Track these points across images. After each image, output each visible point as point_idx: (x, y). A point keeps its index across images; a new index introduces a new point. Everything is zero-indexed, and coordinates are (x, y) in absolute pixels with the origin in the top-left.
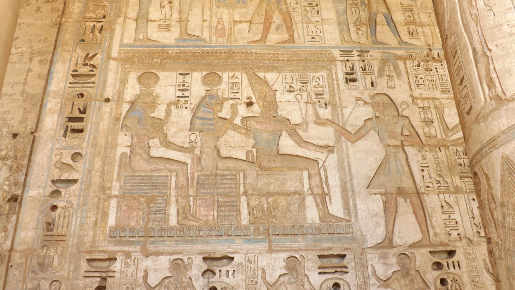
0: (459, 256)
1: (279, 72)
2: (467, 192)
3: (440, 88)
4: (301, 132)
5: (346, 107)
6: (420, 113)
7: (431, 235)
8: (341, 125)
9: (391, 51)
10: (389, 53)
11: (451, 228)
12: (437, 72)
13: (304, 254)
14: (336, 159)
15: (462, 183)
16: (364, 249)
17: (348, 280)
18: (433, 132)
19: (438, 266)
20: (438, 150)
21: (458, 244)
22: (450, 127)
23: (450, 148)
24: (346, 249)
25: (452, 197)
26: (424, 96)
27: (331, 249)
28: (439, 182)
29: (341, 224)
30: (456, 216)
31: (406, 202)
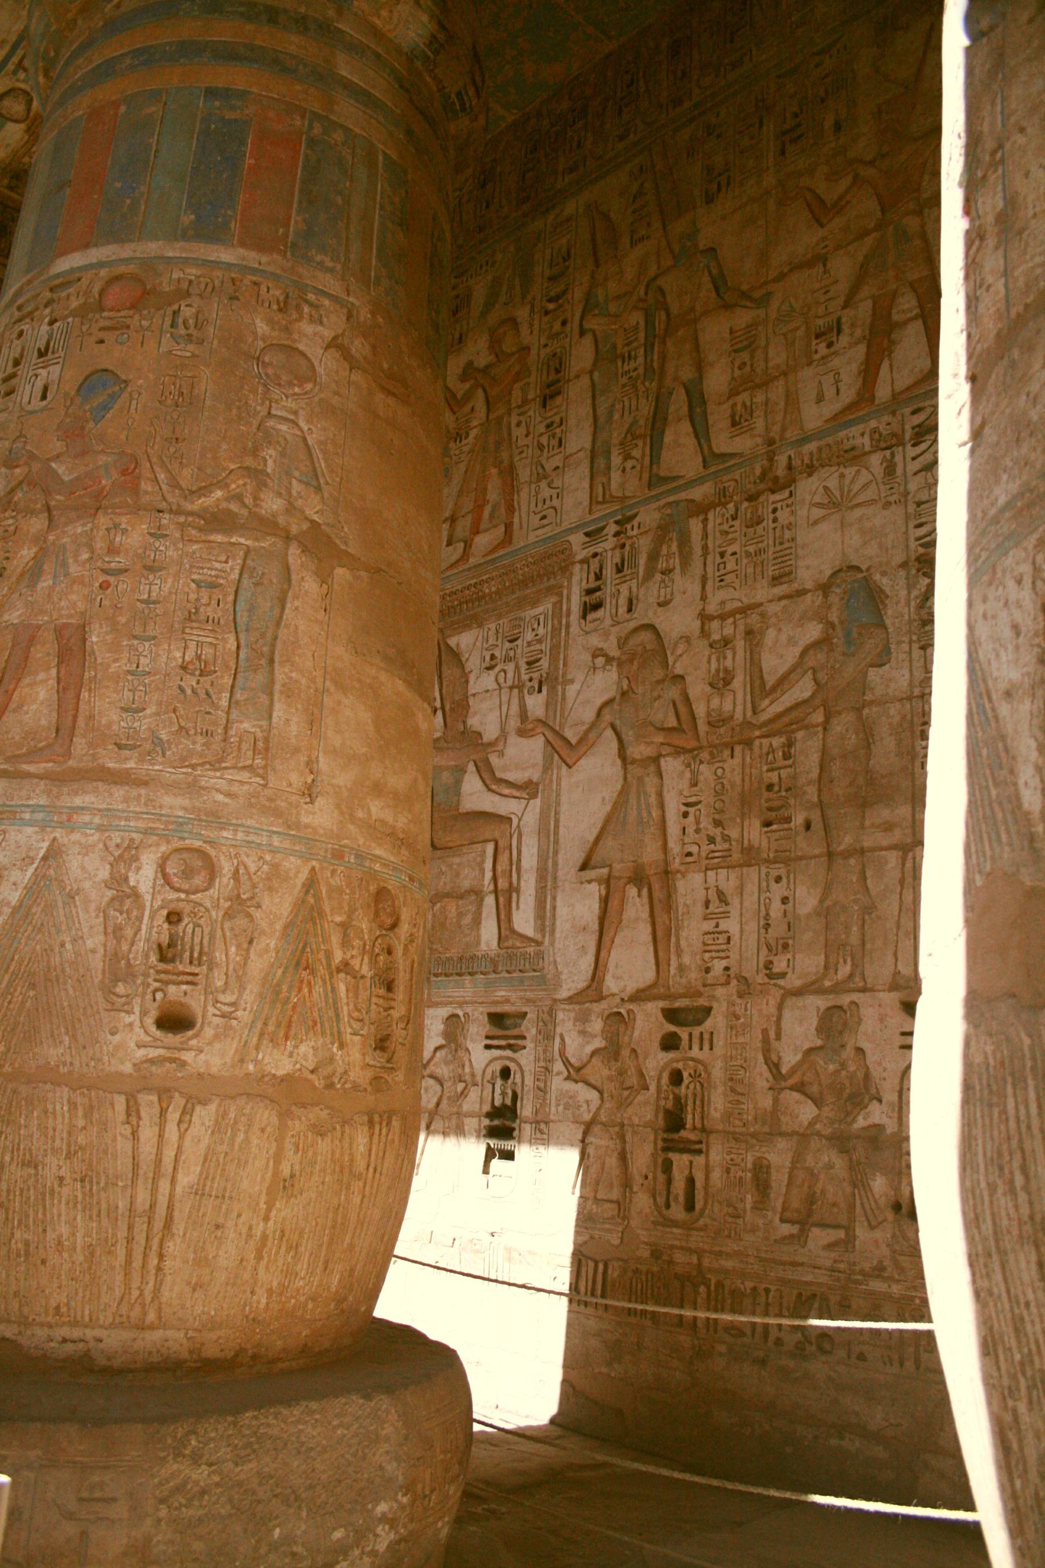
0: (717, 1022)
1: (480, 626)
2: (768, 861)
3: (770, 571)
4: (494, 759)
5: (572, 681)
6: (709, 662)
7: (672, 971)
8: (557, 728)
9: (683, 495)
10: (677, 503)
11: (714, 954)
12: (775, 520)
13: (469, 1009)
14: (538, 810)
15: (764, 837)
16: (555, 1000)
17: (523, 1062)
18: (728, 706)
19: (670, 1043)
20: (727, 753)
21: (720, 992)
22: (770, 681)
23: (757, 742)
24: (528, 1001)
25: (733, 875)
26: (729, 607)
27: (507, 1001)
28: (712, 840)
29: (528, 950)
30: (731, 925)
31: (639, 896)
